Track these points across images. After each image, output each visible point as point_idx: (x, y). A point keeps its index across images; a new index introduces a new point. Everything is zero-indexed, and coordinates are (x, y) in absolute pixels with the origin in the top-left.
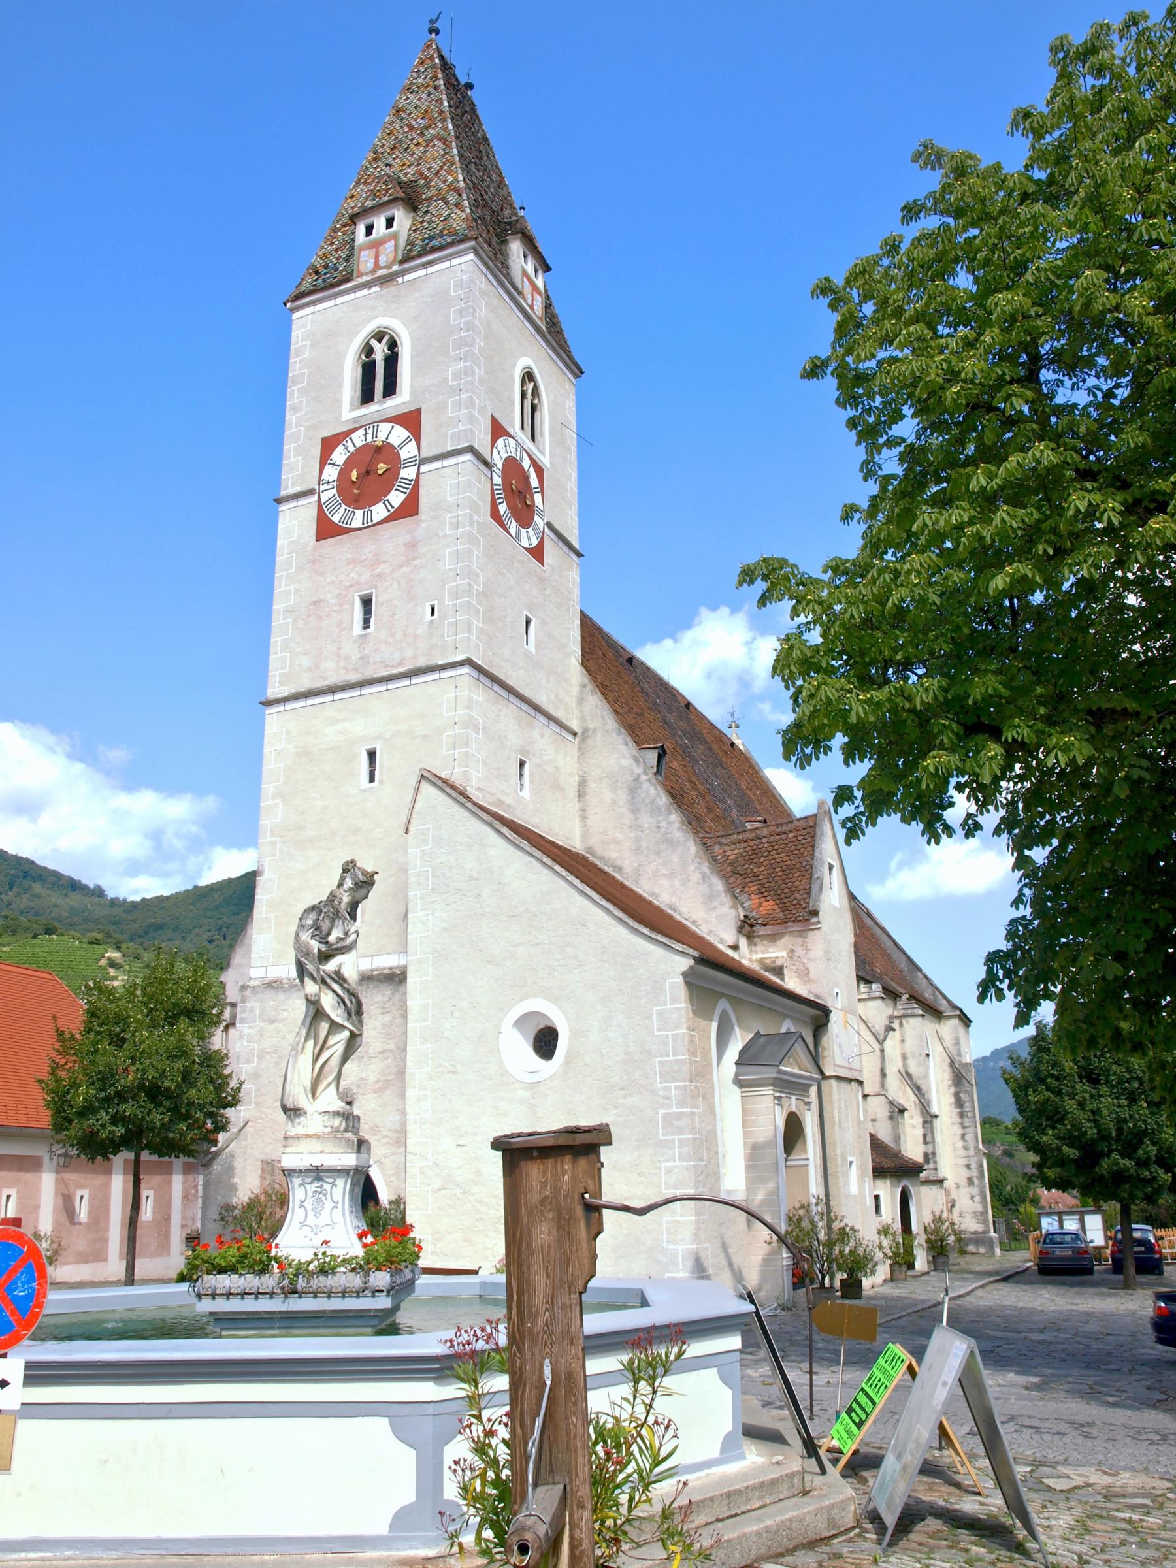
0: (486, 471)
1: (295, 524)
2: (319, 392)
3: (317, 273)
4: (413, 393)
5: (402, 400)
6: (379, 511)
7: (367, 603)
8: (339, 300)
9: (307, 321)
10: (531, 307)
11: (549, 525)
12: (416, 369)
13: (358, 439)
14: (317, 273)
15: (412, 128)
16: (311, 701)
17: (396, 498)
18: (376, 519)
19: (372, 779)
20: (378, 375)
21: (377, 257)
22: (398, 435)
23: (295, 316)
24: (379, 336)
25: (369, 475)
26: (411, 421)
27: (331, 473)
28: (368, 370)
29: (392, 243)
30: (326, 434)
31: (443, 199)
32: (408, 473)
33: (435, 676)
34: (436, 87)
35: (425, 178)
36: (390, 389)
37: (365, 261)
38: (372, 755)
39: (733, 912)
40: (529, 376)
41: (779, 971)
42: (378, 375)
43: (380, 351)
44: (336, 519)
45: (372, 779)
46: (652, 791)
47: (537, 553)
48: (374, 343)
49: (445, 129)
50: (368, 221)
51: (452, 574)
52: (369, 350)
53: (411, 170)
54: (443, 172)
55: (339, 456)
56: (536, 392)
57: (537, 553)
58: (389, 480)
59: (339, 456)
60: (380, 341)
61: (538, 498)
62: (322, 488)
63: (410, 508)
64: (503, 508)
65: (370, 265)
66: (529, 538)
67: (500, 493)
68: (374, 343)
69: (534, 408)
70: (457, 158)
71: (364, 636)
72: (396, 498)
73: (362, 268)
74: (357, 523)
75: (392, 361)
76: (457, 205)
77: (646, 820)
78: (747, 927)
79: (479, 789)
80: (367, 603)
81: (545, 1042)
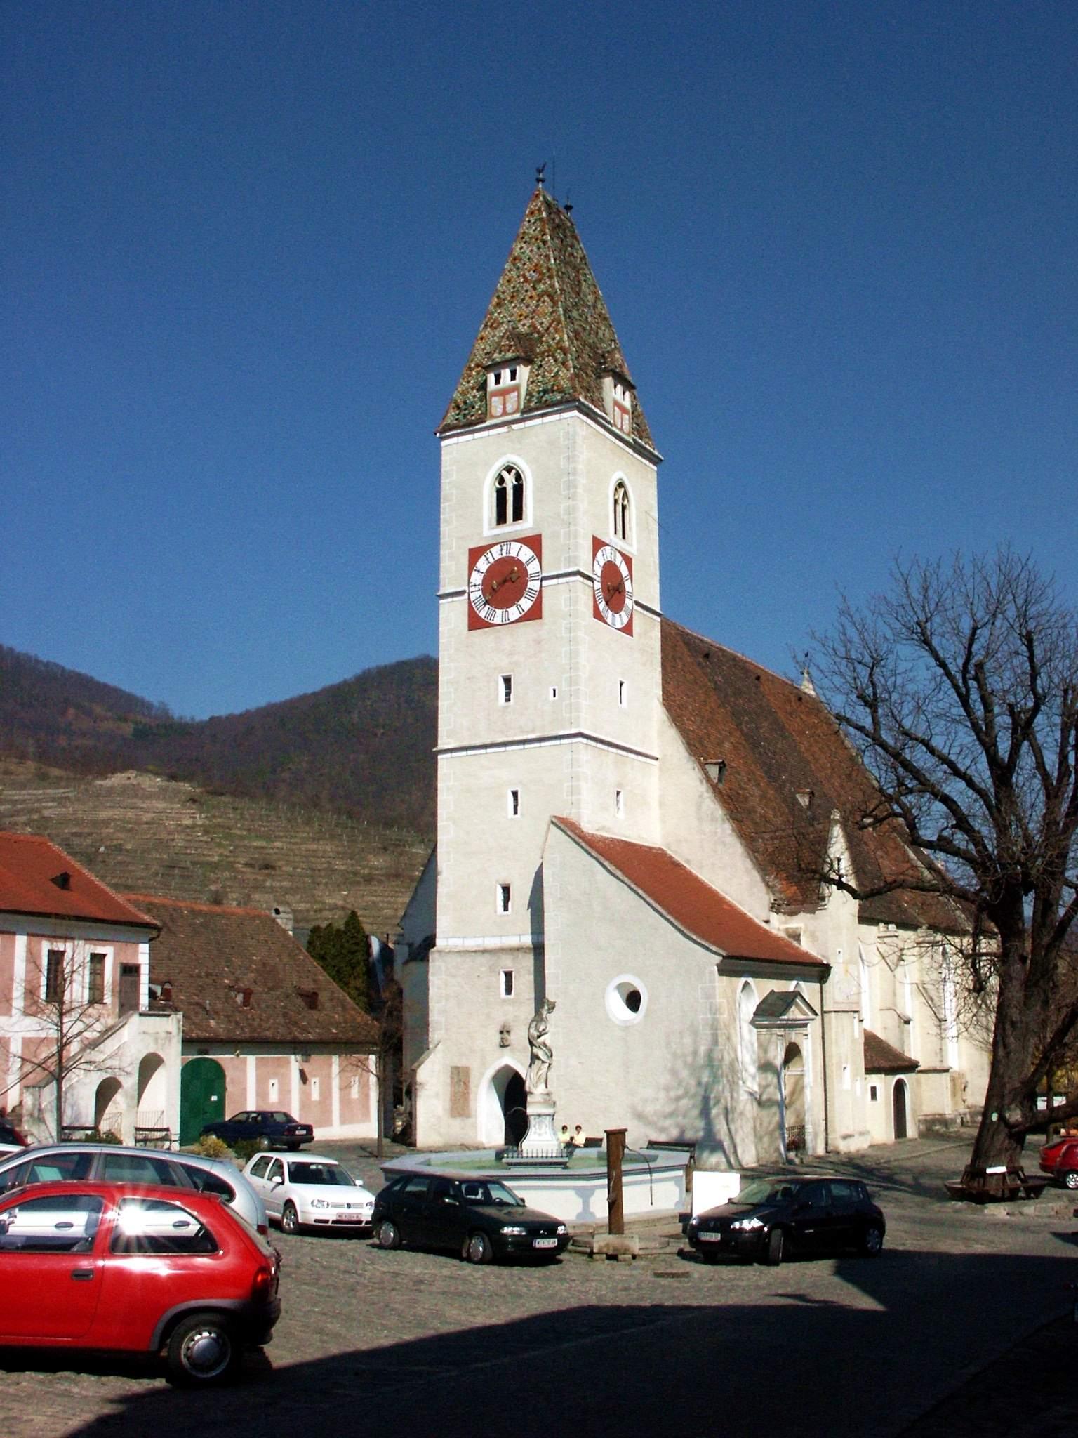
0: (590, 583)
1: (452, 616)
2: (465, 518)
3: (458, 407)
4: (535, 521)
5: (527, 526)
6: (514, 613)
7: (507, 681)
8: (477, 435)
9: (454, 450)
10: (621, 429)
11: (637, 603)
12: (537, 501)
13: (496, 553)
14: (458, 407)
15: (526, 280)
16: (470, 752)
17: (526, 604)
18: (512, 618)
19: (516, 813)
20: (509, 502)
21: (504, 404)
22: (525, 554)
23: (444, 443)
24: (509, 469)
25: (505, 583)
26: (534, 543)
27: (477, 578)
28: (501, 494)
29: (515, 394)
30: (472, 546)
31: (553, 356)
32: (534, 585)
33: (558, 742)
34: (544, 242)
35: (538, 332)
36: (518, 515)
37: (496, 404)
38: (515, 794)
39: (767, 897)
40: (621, 485)
41: (797, 937)
42: (509, 502)
43: (510, 480)
44: (482, 615)
45: (516, 813)
46: (712, 805)
47: (628, 629)
48: (505, 474)
49: (552, 286)
51: (567, 667)
52: (501, 480)
53: (528, 322)
54: (551, 330)
55: (483, 565)
56: (625, 495)
57: (628, 629)
59: (483, 565)
60: (509, 472)
61: (627, 585)
62: (472, 589)
63: (535, 613)
64: (602, 606)
65: (499, 410)
66: (621, 619)
67: (599, 595)
68: (505, 474)
69: (624, 508)
70: (563, 319)
71: (506, 707)
72: (526, 604)
73: (494, 412)
74: (498, 620)
75: (518, 490)
76: (563, 363)
77: (707, 827)
78: (775, 907)
79: (589, 822)
80: (507, 681)
81: (633, 1000)
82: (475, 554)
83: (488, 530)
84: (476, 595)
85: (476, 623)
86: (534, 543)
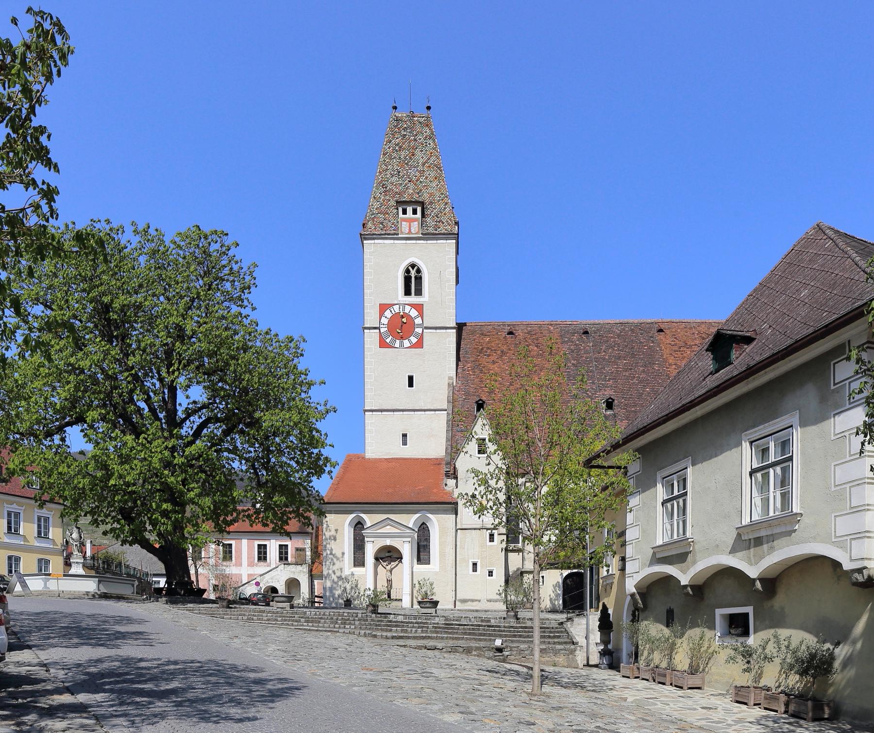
1: (371, 339)
6: (406, 343)
17: (414, 340)
22: (414, 313)
27: (385, 321)
32: (419, 330)
44: (388, 341)
50: (405, 207)
58: (411, 332)
59: (388, 314)
63: (419, 344)
73: (403, 230)
82: (383, 308)
85: (383, 344)
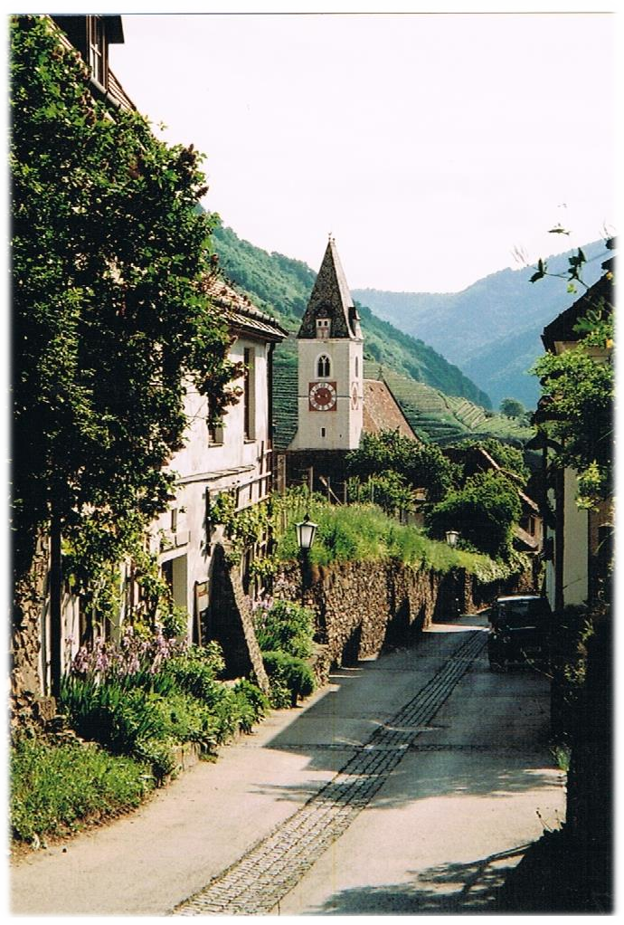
4: (335, 377)
5: (330, 379)
12: (334, 369)
17: (331, 405)
20: (324, 369)
22: (330, 388)
24: (324, 357)
27: (312, 394)
28: (320, 365)
32: (334, 399)
37: (319, 333)
42: (324, 369)
43: (324, 362)
52: (321, 360)
58: (329, 401)
63: (334, 408)
65: (321, 335)
75: (328, 365)
82: (311, 385)
83: (316, 378)
84: (312, 399)
86: (334, 384)
